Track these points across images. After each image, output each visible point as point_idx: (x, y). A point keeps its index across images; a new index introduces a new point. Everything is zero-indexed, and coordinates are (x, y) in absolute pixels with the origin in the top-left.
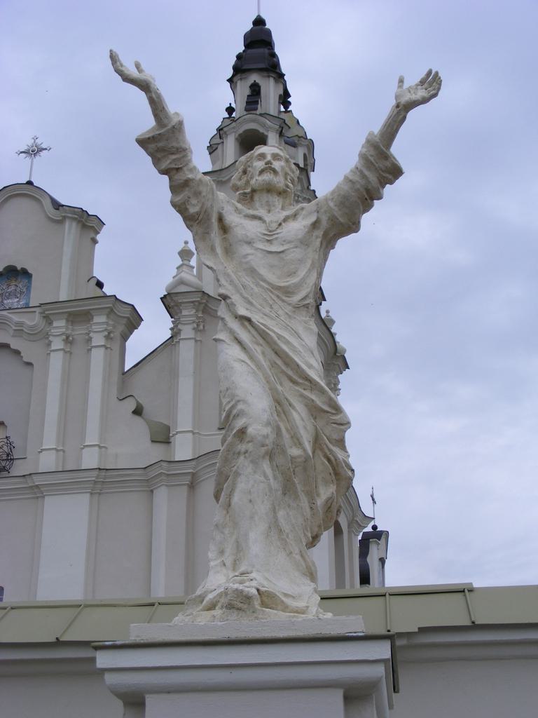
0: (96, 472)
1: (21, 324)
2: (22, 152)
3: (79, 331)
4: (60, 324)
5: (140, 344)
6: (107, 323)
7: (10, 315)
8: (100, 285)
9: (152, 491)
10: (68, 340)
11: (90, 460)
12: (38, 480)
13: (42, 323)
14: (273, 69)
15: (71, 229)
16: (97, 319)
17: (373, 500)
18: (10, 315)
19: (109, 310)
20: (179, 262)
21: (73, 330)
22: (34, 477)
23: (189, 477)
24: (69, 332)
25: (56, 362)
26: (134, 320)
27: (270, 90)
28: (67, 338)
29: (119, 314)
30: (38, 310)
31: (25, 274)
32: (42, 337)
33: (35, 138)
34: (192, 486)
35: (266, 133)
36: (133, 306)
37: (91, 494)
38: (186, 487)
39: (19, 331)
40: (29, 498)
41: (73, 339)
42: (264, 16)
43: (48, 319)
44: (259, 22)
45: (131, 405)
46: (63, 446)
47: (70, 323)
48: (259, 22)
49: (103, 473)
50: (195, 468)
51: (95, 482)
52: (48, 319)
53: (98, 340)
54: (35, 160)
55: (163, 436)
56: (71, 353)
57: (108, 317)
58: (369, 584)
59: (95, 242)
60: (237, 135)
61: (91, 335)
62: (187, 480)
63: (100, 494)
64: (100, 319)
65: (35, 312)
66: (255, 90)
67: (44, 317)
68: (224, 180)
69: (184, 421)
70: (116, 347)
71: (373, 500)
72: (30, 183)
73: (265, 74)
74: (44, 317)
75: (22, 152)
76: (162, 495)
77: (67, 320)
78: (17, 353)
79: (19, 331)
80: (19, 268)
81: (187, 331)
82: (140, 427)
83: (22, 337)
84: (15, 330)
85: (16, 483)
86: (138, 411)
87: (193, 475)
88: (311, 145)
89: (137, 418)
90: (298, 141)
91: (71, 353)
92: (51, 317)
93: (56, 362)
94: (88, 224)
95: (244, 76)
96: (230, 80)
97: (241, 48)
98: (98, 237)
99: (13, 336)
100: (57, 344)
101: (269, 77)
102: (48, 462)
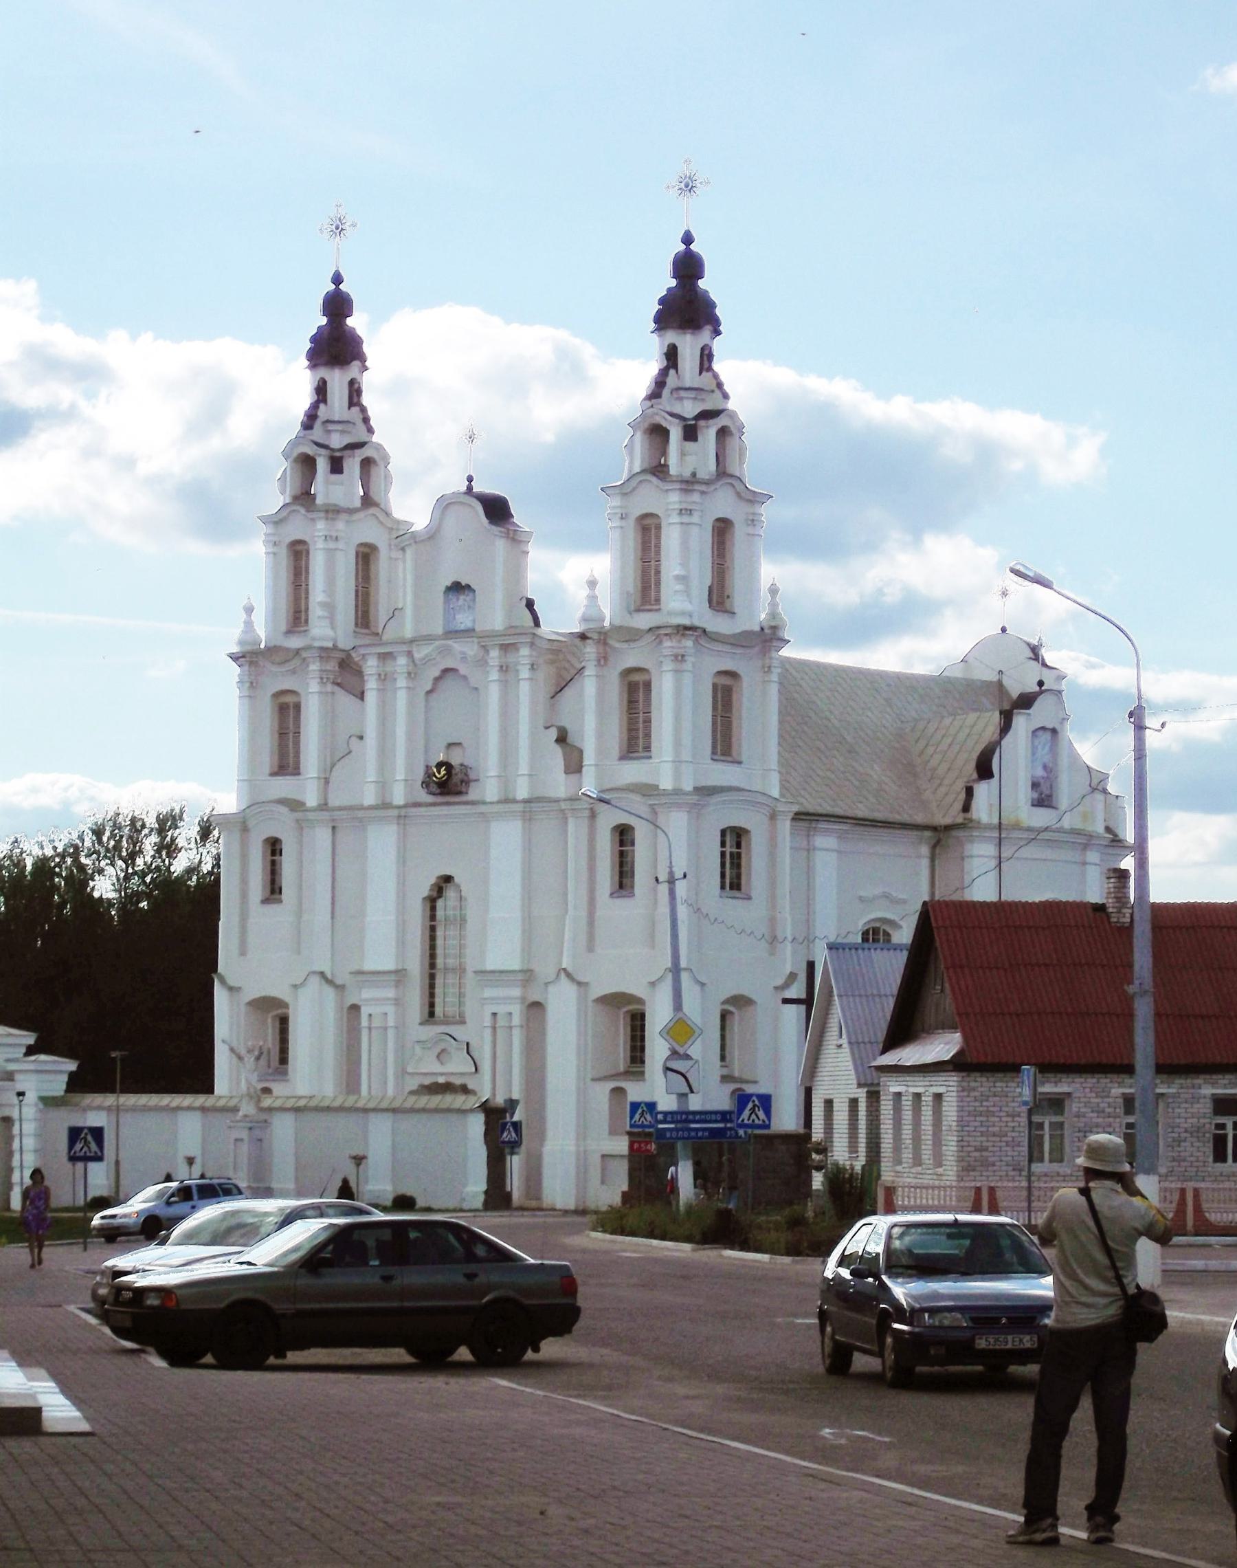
0: (522, 805)
3: (511, 658)
4: (495, 653)
6: (531, 656)
10: (504, 669)
11: (522, 792)
13: (482, 653)
18: (455, 645)
25: (493, 693)
28: (502, 667)
30: (476, 640)
31: (468, 587)
32: (482, 663)
43: (485, 649)
45: (553, 734)
49: (528, 804)
51: (524, 812)
52: (485, 649)
53: (525, 673)
55: (574, 765)
62: (587, 813)
64: (525, 651)
69: (589, 759)
78: (465, 678)
79: (464, 659)
82: (556, 756)
87: (591, 809)
93: (493, 693)
100: (494, 675)
101: (685, 333)
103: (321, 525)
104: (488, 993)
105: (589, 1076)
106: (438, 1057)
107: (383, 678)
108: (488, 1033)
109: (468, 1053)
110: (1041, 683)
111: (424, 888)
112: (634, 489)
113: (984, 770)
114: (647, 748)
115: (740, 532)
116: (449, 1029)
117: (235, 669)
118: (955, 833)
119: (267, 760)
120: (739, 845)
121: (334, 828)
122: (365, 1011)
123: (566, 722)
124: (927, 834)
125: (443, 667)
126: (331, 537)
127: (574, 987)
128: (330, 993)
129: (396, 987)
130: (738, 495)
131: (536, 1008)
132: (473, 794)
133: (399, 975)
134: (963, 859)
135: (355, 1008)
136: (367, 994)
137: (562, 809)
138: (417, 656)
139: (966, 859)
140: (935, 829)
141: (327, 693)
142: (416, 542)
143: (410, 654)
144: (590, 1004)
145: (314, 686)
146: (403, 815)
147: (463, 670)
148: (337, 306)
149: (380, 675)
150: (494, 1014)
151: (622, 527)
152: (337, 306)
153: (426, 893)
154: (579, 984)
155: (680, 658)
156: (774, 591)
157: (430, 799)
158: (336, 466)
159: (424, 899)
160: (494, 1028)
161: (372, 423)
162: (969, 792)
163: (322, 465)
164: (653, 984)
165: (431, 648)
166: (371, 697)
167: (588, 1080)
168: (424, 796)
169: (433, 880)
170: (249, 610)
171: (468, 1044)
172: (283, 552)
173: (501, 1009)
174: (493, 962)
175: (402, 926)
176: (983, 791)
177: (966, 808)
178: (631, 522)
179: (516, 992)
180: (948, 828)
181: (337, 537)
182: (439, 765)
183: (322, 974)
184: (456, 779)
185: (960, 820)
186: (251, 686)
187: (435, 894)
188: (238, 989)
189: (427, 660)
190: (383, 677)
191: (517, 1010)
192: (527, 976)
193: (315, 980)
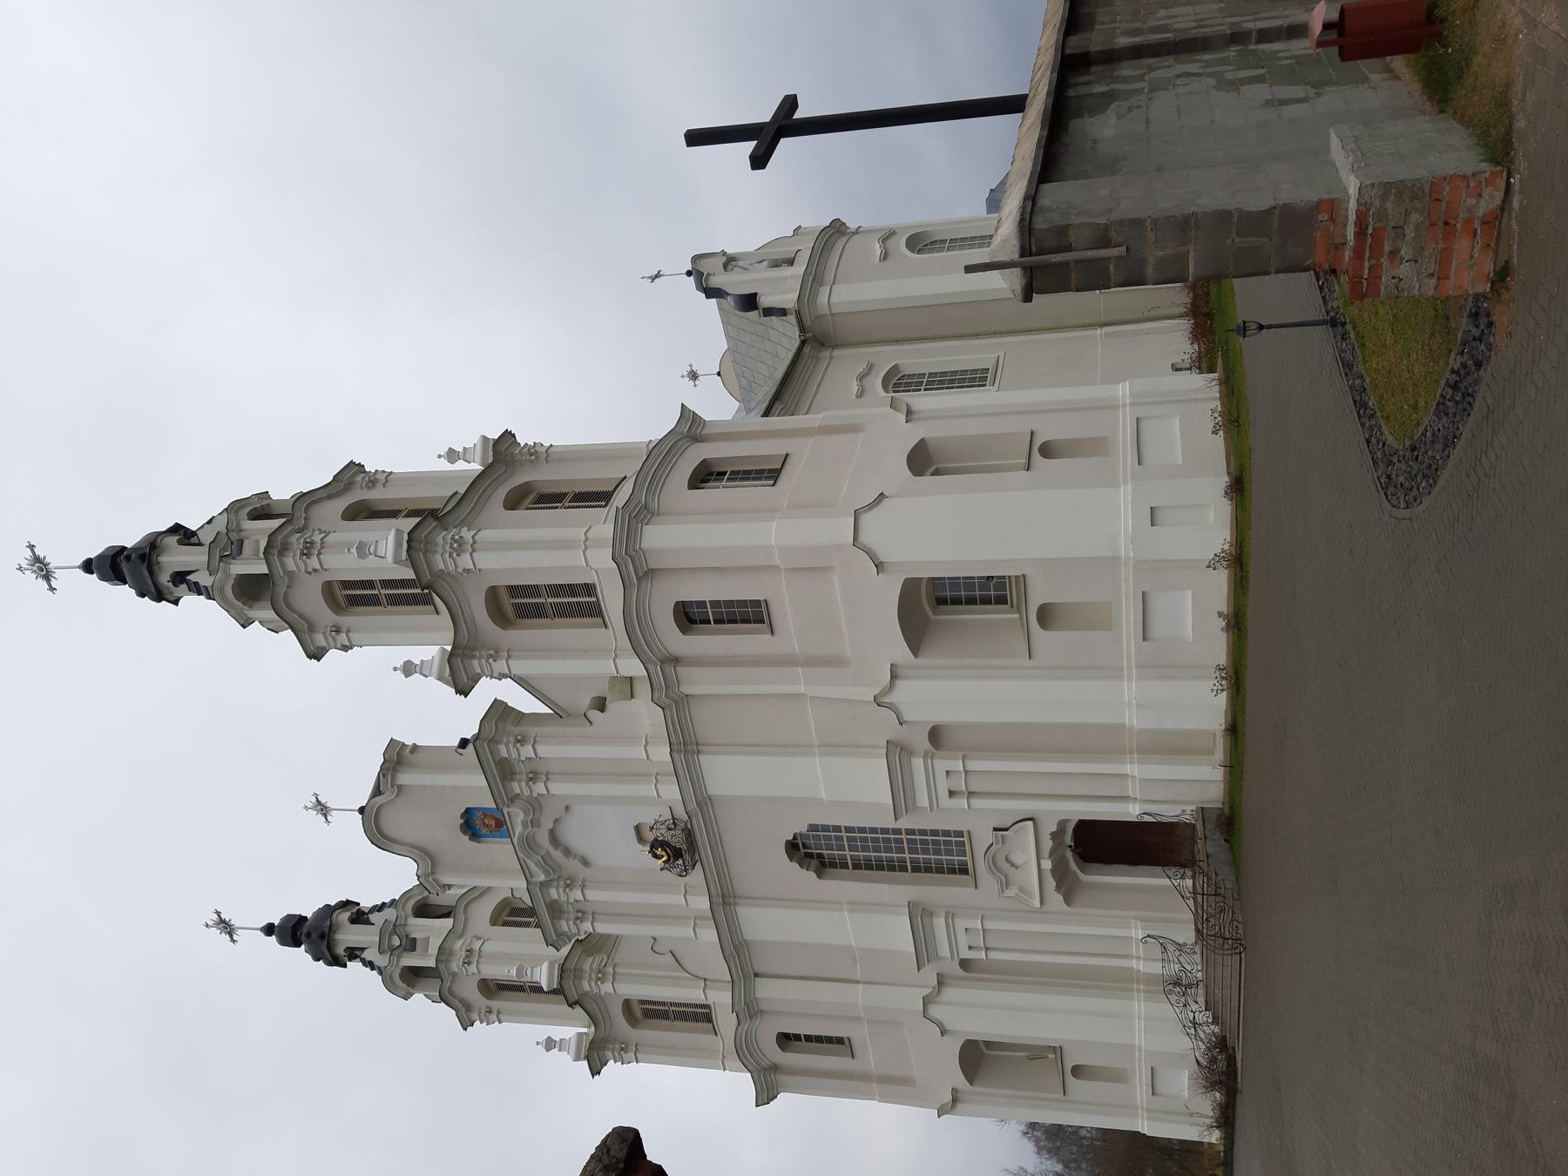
0: (675, 755)
1: (524, 824)
2: (326, 819)
3: (520, 767)
4: (516, 787)
5: (526, 703)
7: (517, 835)
8: (464, 743)
9: (687, 696)
10: (533, 777)
11: (662, 753)
12: (693, 805)
14: (150, 549)
15: (405, 778)
16: (504, 754)
17: (656, 276)
18: (517, 835)
19: (491, 744)
20: (417, 676)
21: (521, 773)
22: (689, 809)
23: (666, 666)
24: (524, 777)
25: (557, 788)
26: (499, 712)
27: (175, 558)
29: (493, 734)
33: (306, 808)
34: (676, 661)
35: (234, 576)
36: (481, 722)
37: (699, 752)
38: (678, 669)
39: (535, 823)
40: (712, 807)
41: (531, 773)
42: (79, 562)
43: (513, 799)
44: (88, 566)
45: (594, 714)
46: (650, 775)
47: (514, 776)
48: (88, 566)
50: (655, 665)
51: (686, 752)
52: (513, 799)
54: (332, 807)
56: (548, 773)
57: (499, 742)
58: (756, 294)
59: (415, 747)
60: (246, 608)
61: (523, 758)
62: (670, 669)
63: (697, 744)
65: (508, 812)
66: (180, 577)
67: (512, 802)
68: (306, 626)
69: (606, 667)
70: (532, 731)
71: (656, 276)
72: (362, 810)
73: (155, 567)
74: (512, 802)
75: (326, 819)
76: (686, 689)
77: (512, 779)
78: (556, 821)
80: (462, 821)
81: (500, 666)
83: (538, 819)
84: (532, 826)
85: (698, 822)
86: (601, 704)
87: (662, 662)
88: (235, 507)
89: (610, 706)
90: (233, 531)
91: (548, 773)
92: (510, 797)
93: (557, 788)
94: (397, 758)
95: (165, 591)
96: (176, 602)
97: (126, 592)
98: (409, 742)
99: (539, 826)
100: (539, 788)
102: (671, 792)
103: (455, 965)
104: (923, 801)
105: (1025, 661)
106: (1017, 867)
107: (581, 915)
108: (978, 803)
109: (1006, 830)
110: (689, 273)
111: (805, 878)
112: (300, 616)
113: (749, 302)
114: (589, 589)
115: (377, 495)
116: (979, 854)
117: (612, 1068)
118: (808, 323)
119: (703, 1039)
120: (724, 473)
121: (756, 975)
122: (966, 954)
123: (585, 700)
124: (807, 349)
125: (551, 849)
126: (467, 956)
127: (900, 683)
128: (949, 993)
129: (931, 914)
130: (330, 497)
131: (936, 735)
132: (681, 813)
133: (919, 916)
134: (832, 315)
135: (965, 964)
136: (944, 950)
137: (675, 705)
138: (542, 878)
139: (834, 311)
140: (803, 343)
141: (614, 972)
142: (433, 873)
143: (544, 885)
144: (919, 661)
145: (606, 988)
146: (724, 901)
147: (547, 824)
148: (292, 931)
149: (578, 918)
150: (952, 793)
151: (348, 631)
152: (292, 931)
153: (812, 875)
154: (894, 676)
155: (459, 546)
156: (452, 456)
157: (698, 865)
158: (411, 945)
159: (819, 877)
160: (970, 794)
161: (387, 901)
162: (769, 312)
163: (411, 960)
164: (879, 566)
165: (528, 861)
166: (602, 928)
167: (1030, 663)
168: (697, 876)
169: (795, 865)
170: (550, 1044)
171: (995, 829)
172: (495, 1004)
173: (943, 786)
174: (882, 794)
175: (855, 906)
176: (765, 301)
177: (782, 312)
178: (345, 620)
179: (918, 763)
180: (802, 329)
181: (467, 951)
182: (656, 856)
183: (926, 1001)
184: (668, 836)
185: (792, 318)
186: (626, 1051)
187: (815, 862)
188: (954, 1091)
189: (548, 864)
190: (580, 914)
191: (941, 765)
192: (898, 753)
193: (935, 1011)
